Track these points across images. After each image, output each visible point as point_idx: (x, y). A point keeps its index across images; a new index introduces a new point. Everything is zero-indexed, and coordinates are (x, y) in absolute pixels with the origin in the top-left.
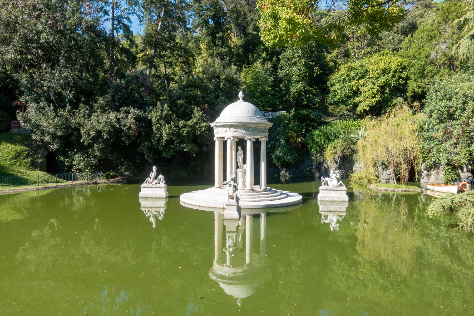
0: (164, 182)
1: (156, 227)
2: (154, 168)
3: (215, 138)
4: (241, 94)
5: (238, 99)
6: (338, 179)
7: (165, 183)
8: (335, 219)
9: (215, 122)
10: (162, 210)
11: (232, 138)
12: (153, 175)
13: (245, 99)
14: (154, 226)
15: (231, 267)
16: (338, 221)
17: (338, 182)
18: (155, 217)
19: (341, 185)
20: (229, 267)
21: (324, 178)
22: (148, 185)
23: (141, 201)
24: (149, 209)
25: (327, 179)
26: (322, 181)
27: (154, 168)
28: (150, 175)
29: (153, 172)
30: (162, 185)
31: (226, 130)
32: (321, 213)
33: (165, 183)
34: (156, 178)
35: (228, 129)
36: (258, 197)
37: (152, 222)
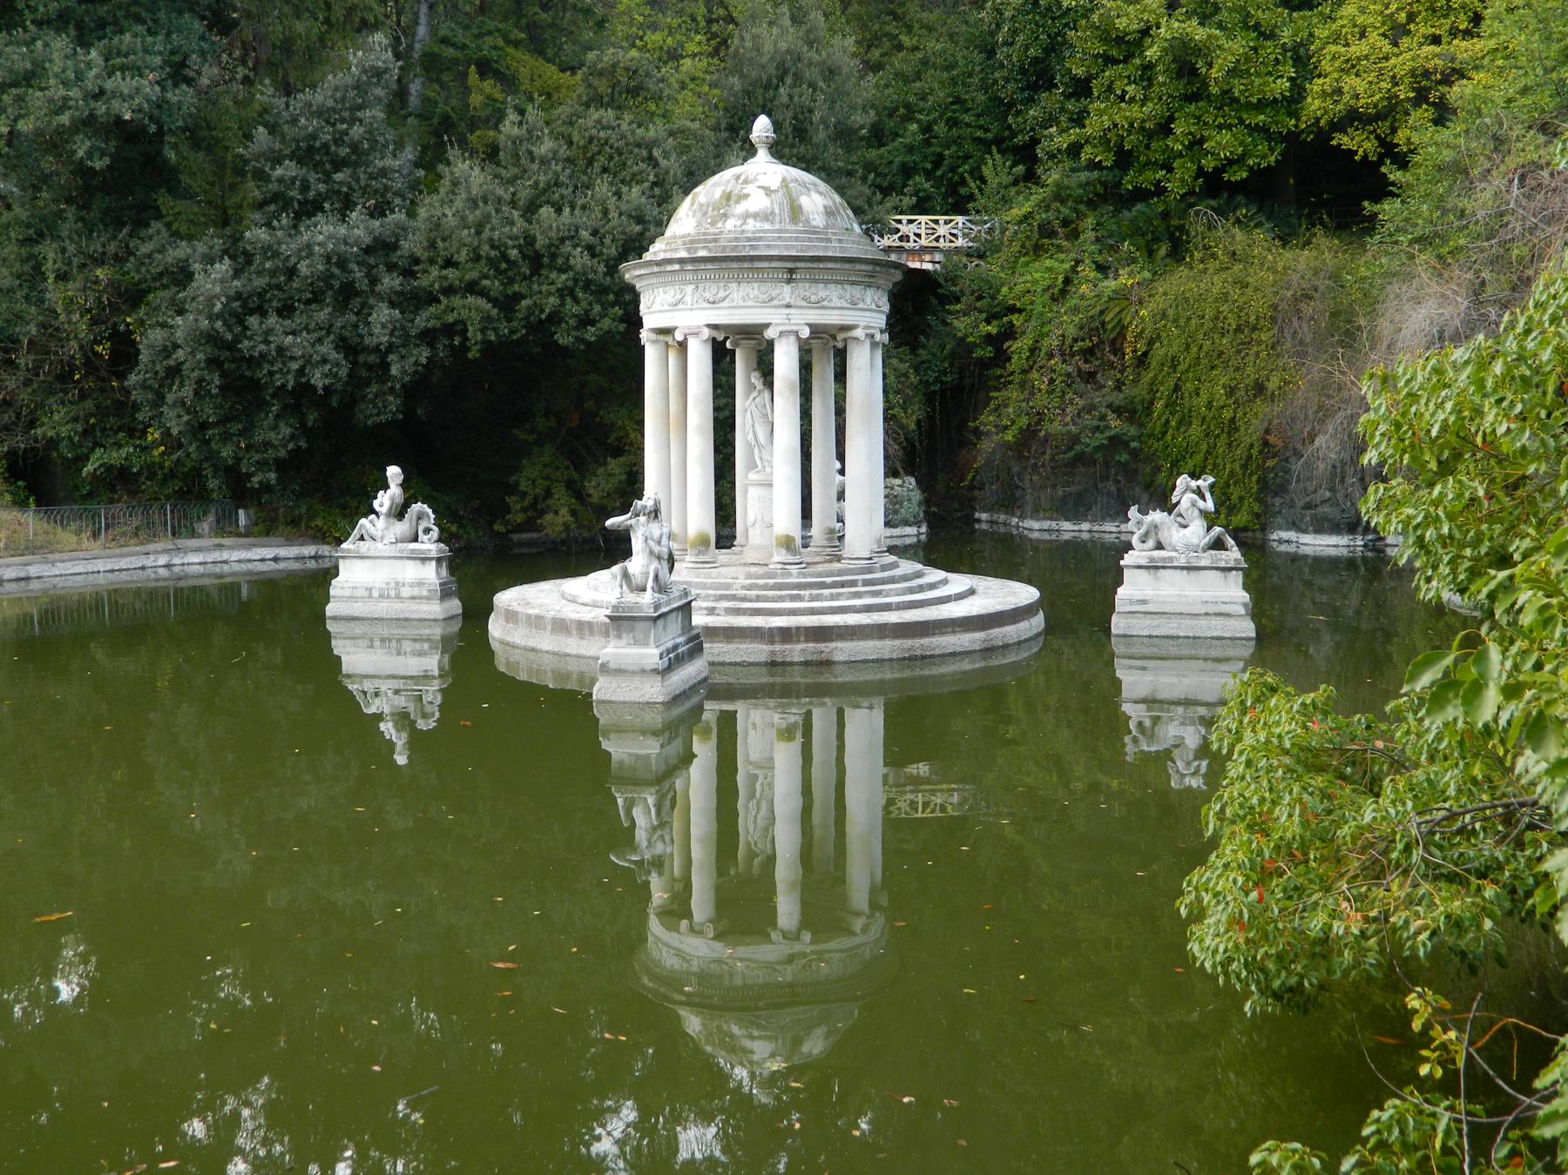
0: (435, 532)
2: (393, 471)
4: (762, 126)
5: (750, 151)
6: (1204, 514)
7: (440, 540)
9: (647, 256)
12: (384, 501)
13: (779, 151)
17: (1209, 529)
19: (1218, 545)
21: (1143, 512)
25: (1157, 516)
27: (393, 471)
28: (376, 504)
29: (386, 487)
30: (429, 545)
31: (678, 297)
33: (440, 540)
34: (399, 513)
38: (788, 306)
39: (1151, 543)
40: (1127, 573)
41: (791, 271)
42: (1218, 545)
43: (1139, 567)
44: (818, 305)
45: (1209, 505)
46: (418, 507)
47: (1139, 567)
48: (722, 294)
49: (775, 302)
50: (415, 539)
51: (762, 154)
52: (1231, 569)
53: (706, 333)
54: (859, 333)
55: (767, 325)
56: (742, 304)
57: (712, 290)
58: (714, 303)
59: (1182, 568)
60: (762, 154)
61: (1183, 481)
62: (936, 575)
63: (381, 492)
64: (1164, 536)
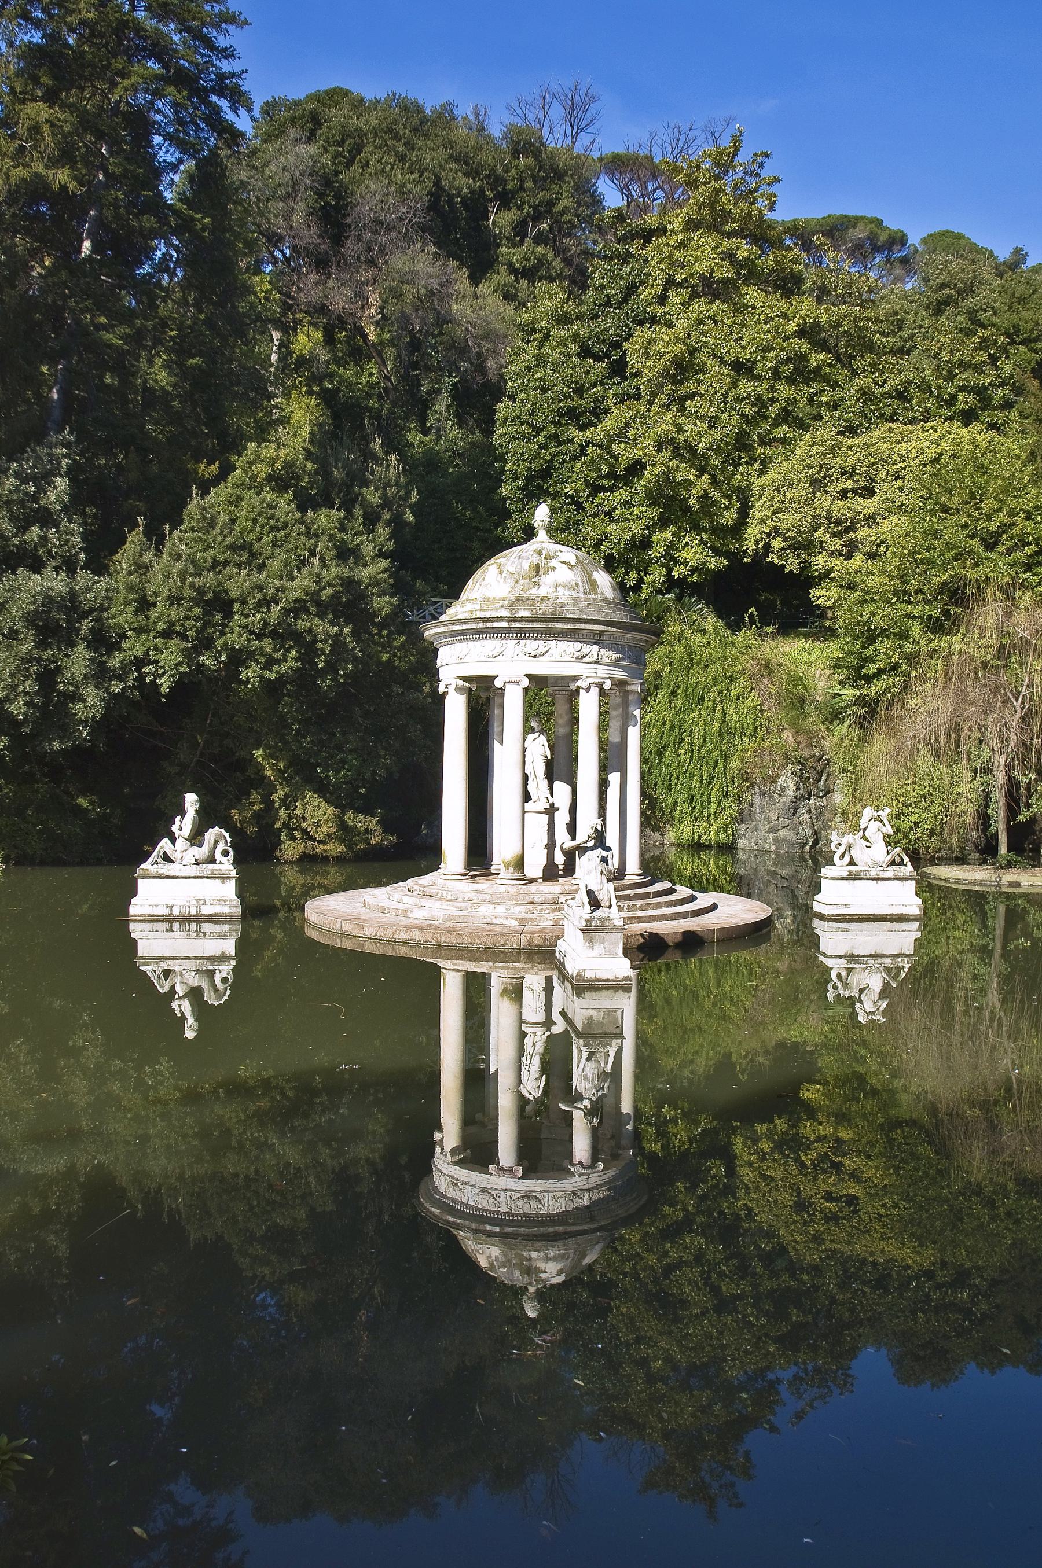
1: (199, 1031)
2: (191, 799)
10: (225, 970)
11: (526, 683)
12: (184, 825)
14: (190, 1034)
16: (885, 992)
18: (195, 994)
20: (510, 1171)
22: (165, 868)
23: (136, 930)
24: (164, 965)
27: (191, 799)
29: (183, 813)
30: (226, 865)
32: (829, 962)
34: (196, 837)
37: (183, 1017)
38: (596, 663)
39: (847, 859)
40: (824, 882)
43: (842, 878)
47: (842, 878)
48: (542, 649)
49: (585, 660)
50: (212, 860)
51: (542, 535)
52: (907, 879)
53: (526, 683)
55: (576, 678)
56: (559, 659)
57: (532, 645)
58: (535, 657)
60: (542, 535)
63: (178, 818)
64: (856, 853)
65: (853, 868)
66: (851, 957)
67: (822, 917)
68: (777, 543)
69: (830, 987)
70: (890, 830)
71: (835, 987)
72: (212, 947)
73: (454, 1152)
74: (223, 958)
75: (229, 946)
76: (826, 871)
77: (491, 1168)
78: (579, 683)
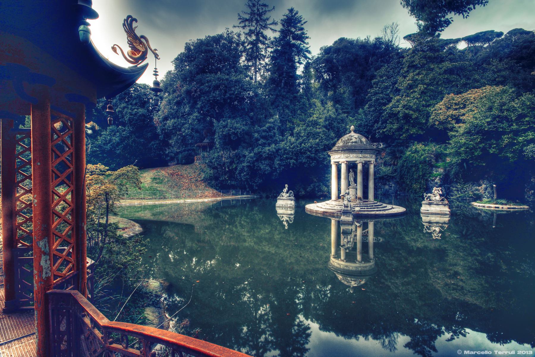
2: (286, 185)
3: (332, 163)
8: (437, 229)
11: (346, 162)
12: (285, 190)
14: (286, 228)
15: (345, 261)
18: (287, 221)
20: (343, 261)
21: (427, 194)
22: (282, 198)
24: (281, 216)
26: (424, 196)
32: (424, 223)
34: (287, 192)
35: (342, 155)
36: (367, 208)
39: (429, 200)
41: (361, 152)
42: (443, 200)
44: (364, 157)
45: (441, 193)
46: (290, 191)
50: (290, 196)
54: (372, 162)
55: (357, 161)
57: (347, 155)
59: (435, 204)
61: (434, 188)
62: (384, 205)
64: (431, 198)
65: (430, 202)
66: (430, 222)
67: (422, 213)
68: (437, 123)
69: (424, 229)
70: (441, 193)
71: (426, 229)
72: (289, 212)
73: (333, 256)
74: (291, 214)
75: (293, 212)
76: (423, 202)
77: (340, 259)
78: (357, 162)
